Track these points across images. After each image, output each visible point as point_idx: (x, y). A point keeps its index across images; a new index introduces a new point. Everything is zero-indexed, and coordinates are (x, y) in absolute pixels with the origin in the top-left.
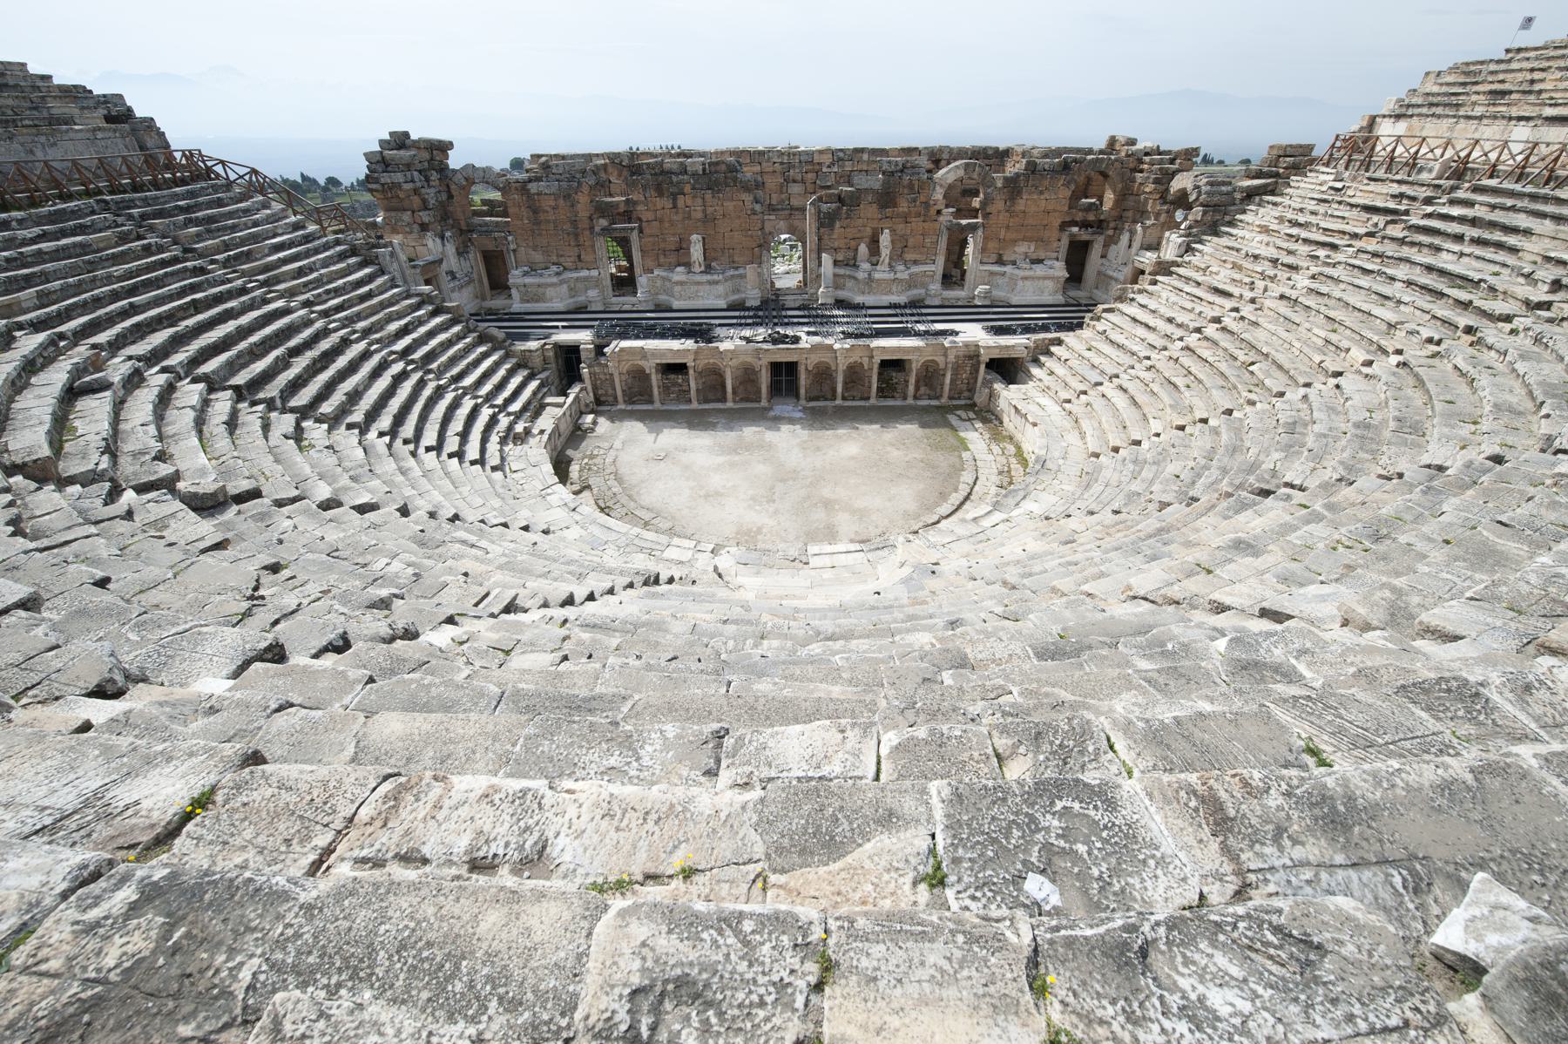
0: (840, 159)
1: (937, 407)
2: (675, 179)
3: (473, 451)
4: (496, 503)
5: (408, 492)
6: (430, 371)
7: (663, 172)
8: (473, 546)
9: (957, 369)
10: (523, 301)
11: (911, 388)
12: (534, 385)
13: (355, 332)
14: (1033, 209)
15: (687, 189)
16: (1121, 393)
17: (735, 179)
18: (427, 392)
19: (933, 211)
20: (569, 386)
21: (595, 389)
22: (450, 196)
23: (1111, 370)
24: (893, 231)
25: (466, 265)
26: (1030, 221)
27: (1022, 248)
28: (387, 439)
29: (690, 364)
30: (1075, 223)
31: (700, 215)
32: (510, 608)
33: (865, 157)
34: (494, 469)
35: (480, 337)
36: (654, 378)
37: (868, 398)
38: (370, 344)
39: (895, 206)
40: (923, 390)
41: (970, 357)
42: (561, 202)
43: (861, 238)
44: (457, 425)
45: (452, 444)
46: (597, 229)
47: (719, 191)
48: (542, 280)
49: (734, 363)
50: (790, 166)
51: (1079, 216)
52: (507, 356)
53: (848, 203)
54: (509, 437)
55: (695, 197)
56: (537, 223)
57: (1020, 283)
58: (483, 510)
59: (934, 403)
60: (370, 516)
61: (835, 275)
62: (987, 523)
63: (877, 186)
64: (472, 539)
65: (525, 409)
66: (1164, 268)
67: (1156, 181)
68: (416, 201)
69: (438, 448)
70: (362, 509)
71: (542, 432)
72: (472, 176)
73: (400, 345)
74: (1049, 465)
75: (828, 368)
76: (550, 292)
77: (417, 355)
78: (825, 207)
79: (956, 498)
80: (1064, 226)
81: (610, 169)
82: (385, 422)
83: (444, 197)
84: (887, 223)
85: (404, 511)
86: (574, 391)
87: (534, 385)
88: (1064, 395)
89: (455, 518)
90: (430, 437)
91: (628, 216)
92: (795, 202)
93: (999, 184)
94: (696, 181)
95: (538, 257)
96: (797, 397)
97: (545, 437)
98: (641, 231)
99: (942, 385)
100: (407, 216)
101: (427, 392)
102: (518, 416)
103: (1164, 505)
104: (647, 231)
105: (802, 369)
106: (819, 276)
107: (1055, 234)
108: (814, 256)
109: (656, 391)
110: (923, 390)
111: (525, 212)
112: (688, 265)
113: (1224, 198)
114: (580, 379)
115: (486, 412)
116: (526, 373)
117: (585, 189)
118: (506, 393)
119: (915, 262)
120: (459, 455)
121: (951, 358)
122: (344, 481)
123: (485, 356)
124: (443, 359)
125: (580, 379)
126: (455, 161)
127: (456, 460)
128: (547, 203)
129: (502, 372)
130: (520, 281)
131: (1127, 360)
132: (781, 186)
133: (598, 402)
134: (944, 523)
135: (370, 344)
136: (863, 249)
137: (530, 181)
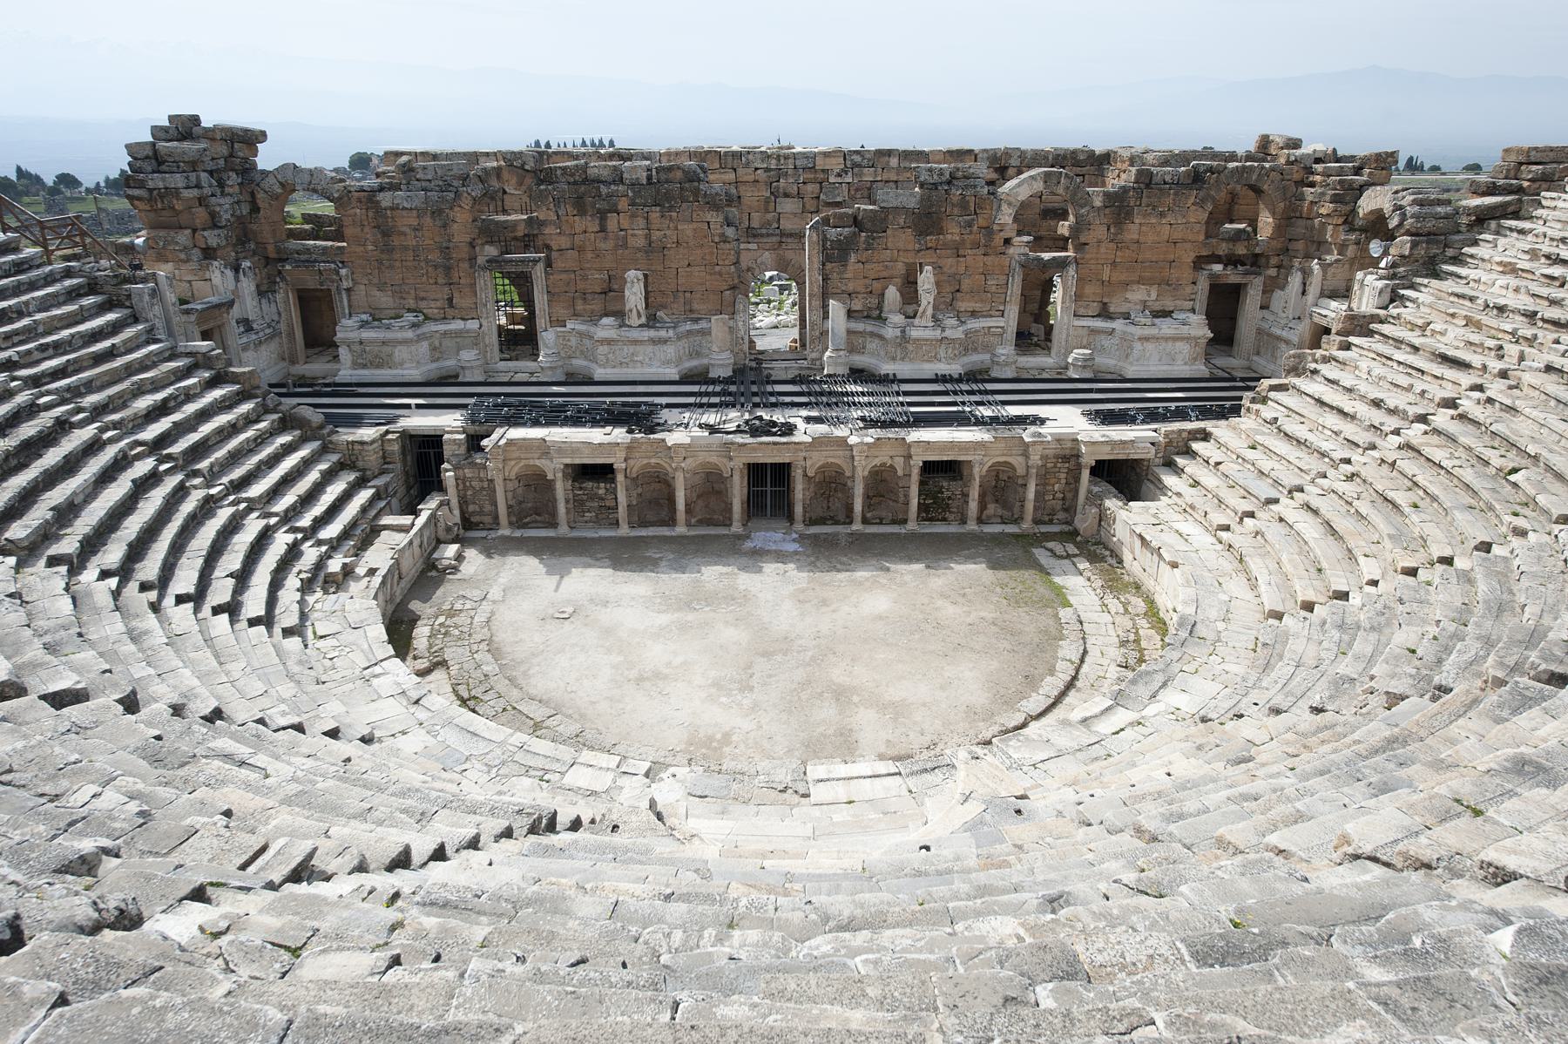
0: (855, 165)
1: (1016, 536)
2: (604, 190)
3: (254, 603)
4: (287, 689)
5: (140, 671)
6: (196, 473)
7: (586, 181)
8: (242, 764)
9: (1044, 477)
10: (356, 365)
11: (973, 506)
12: (364, 495)
13: (79, 410)
14: (1151, 238)
15: (623, 204)
16: (1309, 516)
18: (188, 506)
19: (998, 240)
21: (463, 502)
22: (255, 209)
23: (1290, 480)
24: (938, 268)
25: (270, 310)
26: (1148, 255)
27: (1137, 294)
28: (113, 582)
29: (619, 465)
30: (1216, 259)
32: (302, 873)
33: (894, 162)
34: (288, 632)
35: (283, 420)
37: (905, 521)
38: (102, 430)
39: (940, 231)
40: (992, 508)
41: (1065, 459)
42: (428, 220)
43: (889, 279)
44: (232, 560)
45: (221, 591)
46: (481, 260)
47: (671, 209)
48: (389, 335)
49: (689, 464)
50: (781, 173)
51: (1223, 249)
52: (324, 450)
53: (868, 228)
54: (319, 579)
55: (633, 216)
56: (388, 249)
57: (1138, 346)
58: (265, 702)
59: (1011, 529)
60: (73, 712)
61: (849, 332)
63: (912, 203)
64: (243, 751)
65: (346, 534)
66: (1360, 325)
68: (201, 214)
69: (197, 598)
70: (59, 700)
71: (372, 572)
72: (292, 180)
73: (151, 432)
74: (1201, 630)
75: (840, 473)
76: (400, 353)
77: (177, 448)
78: (832, 233)
79: (1052, 686)
81: (505, 175)
82: (113, 554)
83: (245, 209)
84: (928, 256)
85: (130, 704)
86: (428, 507)
87: (364, 495)
88: (1219, 518)
89: (216, 715)
90: (185, 580)
91: (527, 242)
92: (787, 225)
93: (1098, 202)
94: (637, 194)
95: (385, 300)
96: (790, 518)
97: (377, 580)
98: (549, 264)
99: (1023, 501)
100: (183, 237)
101: (188, 506)
102: (334, 545)
103: (1394, 699)
104: (559, 264)
105: (797, 475)
106: (824, 333)
107: (1187, 274)
108: (817, 303)
109: (562, 508)
110: (992, 508)
111: (370, 234)
112: (620, 314)
113: (1441, 224)
114: (440, 487)
115: (282, 540)
116: (352, 477)
117: (466, 203)
118: (318, 510)
119: (974, 314)
120: (231, 609)
121: (1035, 459)
122: (35, 652)
123: (288, 449)
124: (220, 453)
125: (440, 487)
126: (267, 158)
127: (225, 617)
128: (406, 222)
129: (314, 476)
130: (354, 335)
131: (1314, 464)
132: (767, 201)
133: (467, 523)
134: (1033, 725)
135: (102, 430)
136: (892, 294)
137: (381, 189)
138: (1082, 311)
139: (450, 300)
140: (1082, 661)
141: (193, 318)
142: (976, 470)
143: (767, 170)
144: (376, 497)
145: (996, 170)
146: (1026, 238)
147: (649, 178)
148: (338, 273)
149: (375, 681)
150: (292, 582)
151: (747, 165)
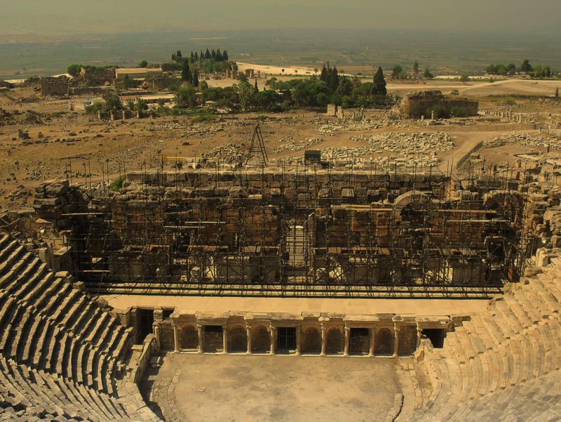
9: (401, 335)
12: (125, 336)
20: (144, 337)
38: (42, 315)
44: (89, 369)
65: (120, 354)
66: (535, 274)
67: (535, 212)
73: (55, 316)
74: (435, 408)
82: (59, 368)
87: (125, 336)
97: (133, 374)
105: (298, 331)
137: (129, 199)
140: (397, 415)
141: (58, 259)
142: (373, 332)
149: (141, 415)
150: (108, 376)
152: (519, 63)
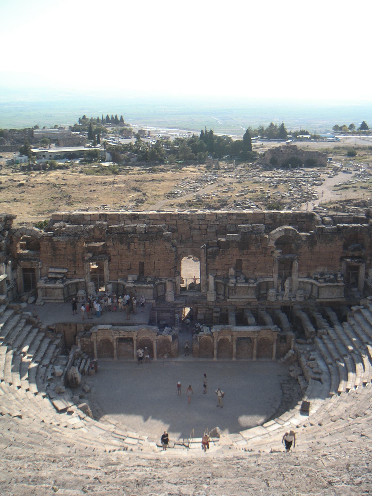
12: (53, 347)
15: (136, 240)
17: (162, 236)
19: (269, 252)
29: (135, 338)
31: (142, 253)
33: (234, 217)
35: (26, 322)
36: (115, 344)
39: (248, 248)
42: (69, 246)
46: (86, 258)
47: (153, 241)
51: (351, 253)
55: (140, 244)
62: (270, 429)
63: (238, 239)
80: (342, 259)
83: (9, 242)
87: (53, 347)
92: (195, 238)
93: (304, 239)
98: (109, 261)
123: (30, 332)
126: (15, 225)
138: (300, 276)
139: (75, 272)
142: (255, 340)
143: (188, 220)
144: (57, 347)
145: (272, 220)
146: (279, 251)
147: (145, 231)
148: (38, 263)
151: (180, 219)
152: (358, 125)
